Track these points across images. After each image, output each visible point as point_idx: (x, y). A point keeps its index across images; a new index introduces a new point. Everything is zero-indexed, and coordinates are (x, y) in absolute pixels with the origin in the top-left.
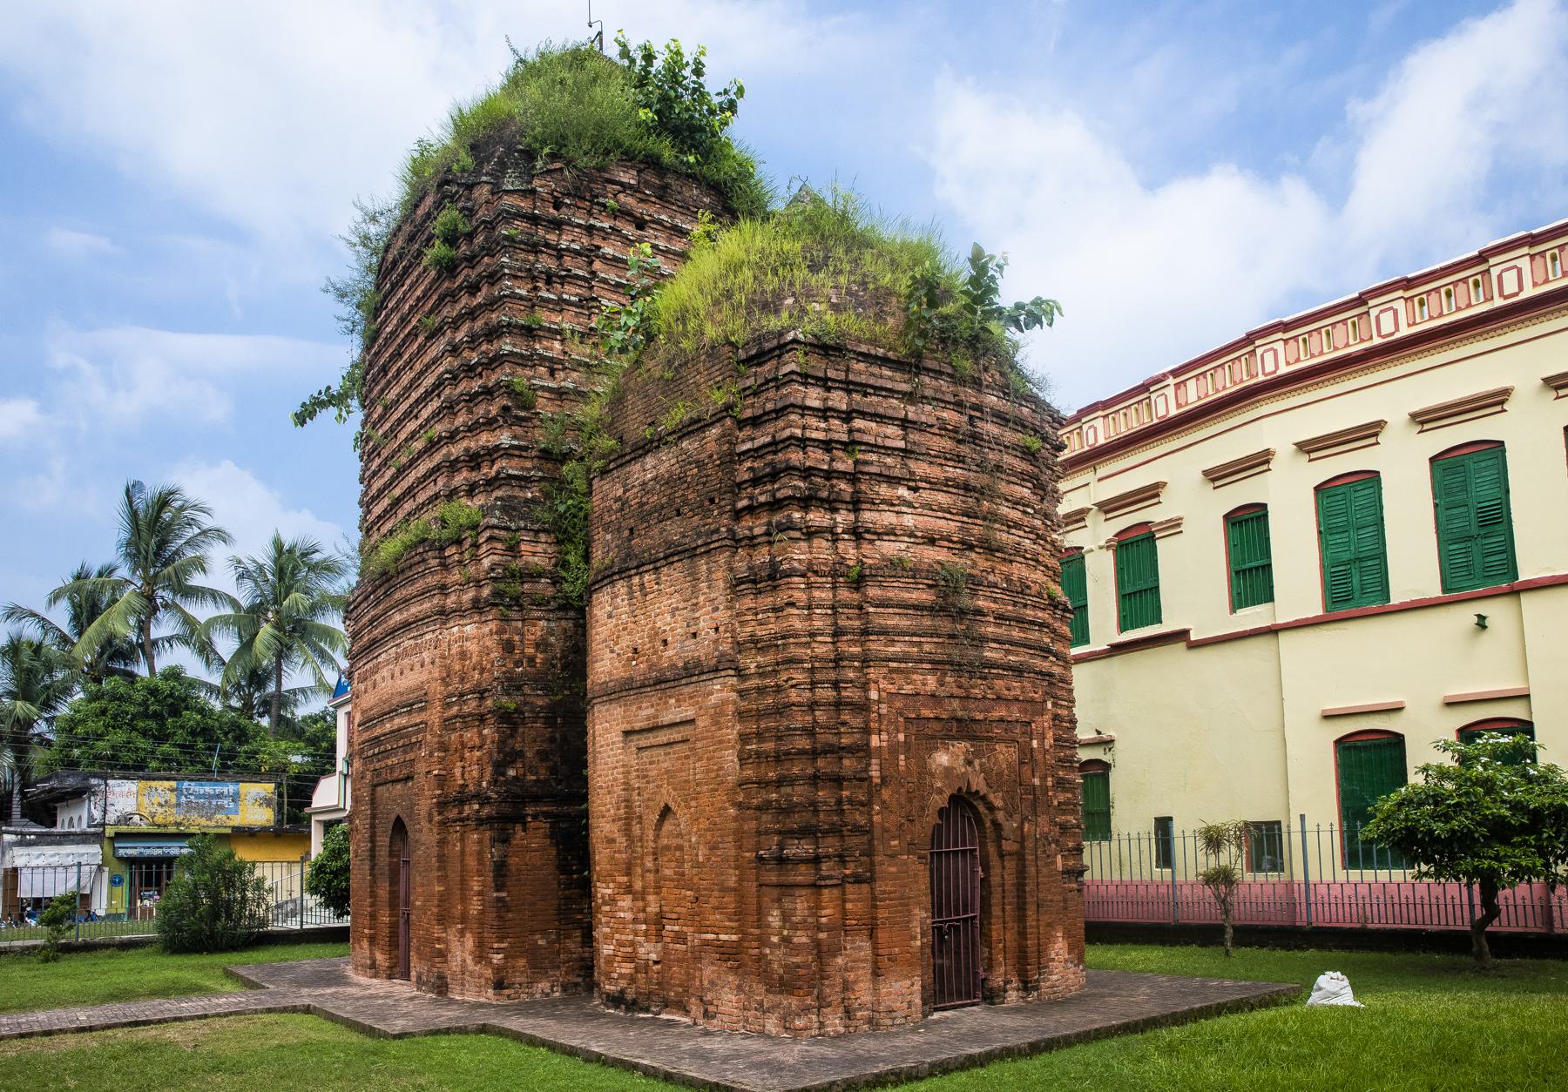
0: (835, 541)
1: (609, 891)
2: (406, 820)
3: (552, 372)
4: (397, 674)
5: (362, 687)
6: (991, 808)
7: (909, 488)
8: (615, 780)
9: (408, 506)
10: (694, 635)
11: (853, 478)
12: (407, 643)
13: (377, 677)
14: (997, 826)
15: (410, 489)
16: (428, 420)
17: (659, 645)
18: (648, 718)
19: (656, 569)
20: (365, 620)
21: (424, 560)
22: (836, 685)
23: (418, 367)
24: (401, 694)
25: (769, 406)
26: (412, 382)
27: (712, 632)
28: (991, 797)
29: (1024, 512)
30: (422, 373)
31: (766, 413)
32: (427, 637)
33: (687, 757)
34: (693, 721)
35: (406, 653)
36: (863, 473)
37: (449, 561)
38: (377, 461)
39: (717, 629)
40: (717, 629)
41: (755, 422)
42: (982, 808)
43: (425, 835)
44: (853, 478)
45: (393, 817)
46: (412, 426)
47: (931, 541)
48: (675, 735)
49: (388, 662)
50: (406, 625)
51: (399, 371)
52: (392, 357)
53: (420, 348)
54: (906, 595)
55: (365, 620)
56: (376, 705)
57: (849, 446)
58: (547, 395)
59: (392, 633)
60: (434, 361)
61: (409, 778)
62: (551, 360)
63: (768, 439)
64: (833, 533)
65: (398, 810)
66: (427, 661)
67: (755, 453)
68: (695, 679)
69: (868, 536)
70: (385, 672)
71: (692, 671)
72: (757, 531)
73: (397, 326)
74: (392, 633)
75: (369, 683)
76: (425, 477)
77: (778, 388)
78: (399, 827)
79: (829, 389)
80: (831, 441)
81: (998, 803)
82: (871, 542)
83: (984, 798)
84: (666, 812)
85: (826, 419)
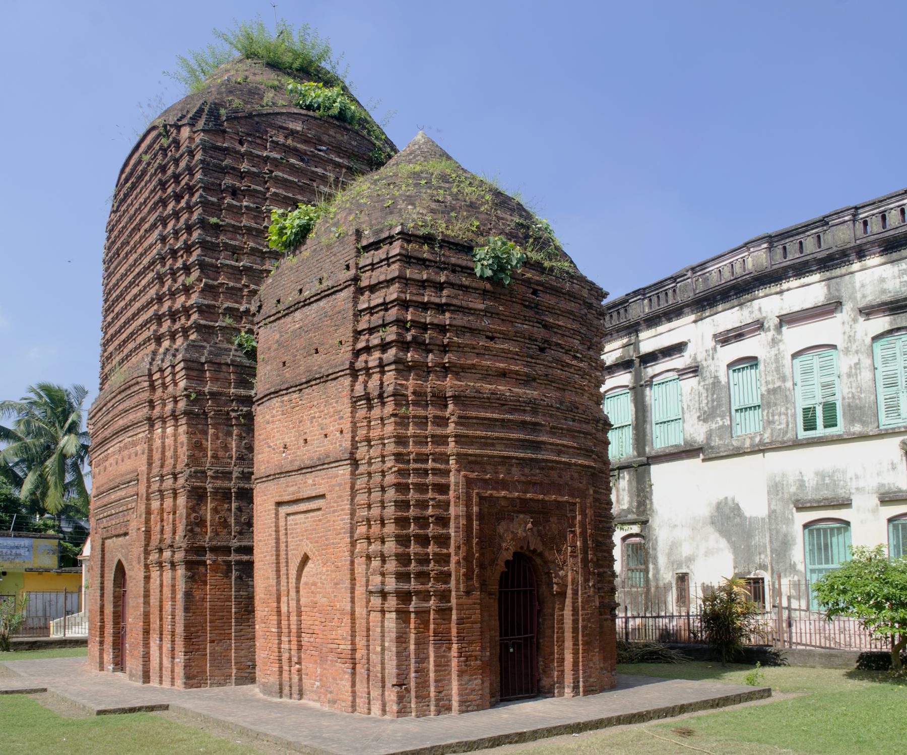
1: (265, 613)
2: (124, 563)
4: (120, 461)
5: (97, 470)
9: (131, 346)
10: (326, 436)
12: (127, 440)
13: (107, 463)
15: (132, 334)
16: (145, 287)
17: (302, 442)
18: (293, 494)
19: (300, 390)
20: (100, 424)
23: (140, 250)
24: (122, 475)
25: (382, 278)
26: (136, 261)
27: (338, 434)
30: (142, 255)
31: (380, 283)
32: (140, 436)
33: (320, 520)
35: (126, 447)
37: (156, 383)
38: (112, 315)
39: (341, 432)
40: (341, 432)
41: (373, 288)
43: (135, 574)
46: (135, 291)
49: (114, 453)
50: (125, 429)
51: (127, 254)
52: (123, 244)
53: (141, 238)
55: (100, 424)
56: (106, 483)
58: (230, 271)
59: (116, 433)
60: (150, 247)
61: (126, 534)
63: (381, 301)
65: (120, 556)
66: (139, 452)
67: (371, 310)
68: (326, 466)
70: (112, 460)
72: (371, 364)
73: (127, 223)
74: (116, 433)
75: (101, 467)
76: (142, 326)
77: (389, 265)
78: (120, 570)
84: (305, 559)
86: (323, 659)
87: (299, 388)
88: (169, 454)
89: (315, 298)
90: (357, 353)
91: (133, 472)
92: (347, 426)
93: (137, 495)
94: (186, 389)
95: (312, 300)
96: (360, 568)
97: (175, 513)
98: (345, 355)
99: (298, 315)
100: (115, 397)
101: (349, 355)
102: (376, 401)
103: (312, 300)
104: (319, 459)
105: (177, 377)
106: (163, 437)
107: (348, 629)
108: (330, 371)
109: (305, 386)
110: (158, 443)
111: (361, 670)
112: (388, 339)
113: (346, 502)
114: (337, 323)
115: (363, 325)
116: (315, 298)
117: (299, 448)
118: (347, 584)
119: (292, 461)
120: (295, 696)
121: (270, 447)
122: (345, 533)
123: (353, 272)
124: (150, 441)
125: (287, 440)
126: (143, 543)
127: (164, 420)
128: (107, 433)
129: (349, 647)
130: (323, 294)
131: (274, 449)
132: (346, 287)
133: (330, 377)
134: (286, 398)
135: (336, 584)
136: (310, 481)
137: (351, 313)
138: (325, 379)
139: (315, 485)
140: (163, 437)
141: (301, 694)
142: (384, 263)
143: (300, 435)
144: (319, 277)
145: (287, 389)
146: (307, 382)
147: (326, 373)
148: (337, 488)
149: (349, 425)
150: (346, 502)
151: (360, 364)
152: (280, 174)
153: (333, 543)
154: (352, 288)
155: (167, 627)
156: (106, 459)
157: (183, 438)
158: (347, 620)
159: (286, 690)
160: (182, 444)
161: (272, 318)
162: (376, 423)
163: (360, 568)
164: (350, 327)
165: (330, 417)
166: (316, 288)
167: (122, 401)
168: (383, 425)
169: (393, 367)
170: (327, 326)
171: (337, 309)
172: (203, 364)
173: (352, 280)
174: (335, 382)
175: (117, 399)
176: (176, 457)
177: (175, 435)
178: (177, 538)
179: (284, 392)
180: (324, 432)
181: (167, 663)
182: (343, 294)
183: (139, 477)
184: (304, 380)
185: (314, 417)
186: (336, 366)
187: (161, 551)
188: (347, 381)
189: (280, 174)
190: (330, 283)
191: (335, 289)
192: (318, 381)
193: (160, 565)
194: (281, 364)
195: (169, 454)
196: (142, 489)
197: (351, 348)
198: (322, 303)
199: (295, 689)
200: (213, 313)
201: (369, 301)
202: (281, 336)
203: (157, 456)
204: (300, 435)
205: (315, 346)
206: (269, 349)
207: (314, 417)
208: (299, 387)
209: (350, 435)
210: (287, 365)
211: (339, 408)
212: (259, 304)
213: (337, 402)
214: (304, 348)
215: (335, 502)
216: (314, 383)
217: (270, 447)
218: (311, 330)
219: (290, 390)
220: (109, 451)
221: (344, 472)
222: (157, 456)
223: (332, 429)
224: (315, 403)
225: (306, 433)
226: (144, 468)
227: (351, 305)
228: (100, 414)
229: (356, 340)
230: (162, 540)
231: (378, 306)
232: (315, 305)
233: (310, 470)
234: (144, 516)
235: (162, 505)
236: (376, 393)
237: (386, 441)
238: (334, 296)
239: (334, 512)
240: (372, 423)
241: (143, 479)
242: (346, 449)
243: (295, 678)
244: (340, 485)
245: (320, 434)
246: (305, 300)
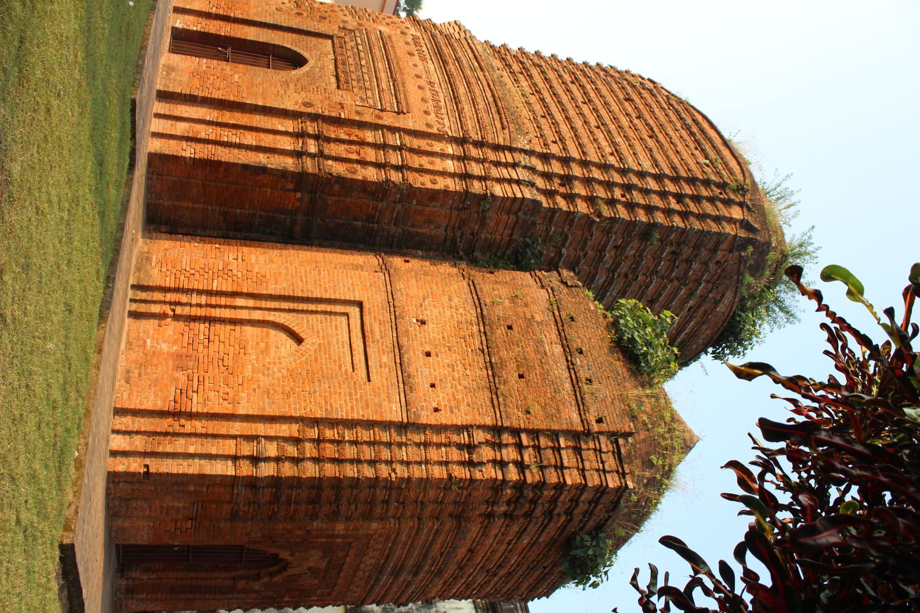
0: (487, 502)
3: (616, 247)
6: (271, 575)
7: (511, 540)
8: (326, 291)
9: (538, 108)
10: (433, 386)
11: (528, 515)
13: (417, 58)
14: (258, 577)
17: (427, 349)
19: (483, 351)
21: (503, 128)
22: (386, 502)
27: (435, 405)
28: (281, 576)
29: (474, 589)
31: (582, 461)
32: (446, 121)
34: (369, 380)
36: (530, 521)
39: (436, 410)
40: (436, 410)
42: (272, 569)
44: (528, 515)
45: (306, 55)
47: (471, 550)
48: (359, 357)
54: (440, 541)
57: (549, 514)
58: (603, 242)
62: (625, 248)
63: (566, 464)
64: (493, 503)
65: (311, 63)
68: (401, 385)
69: (486, 521)
71: (406, 382)
78: (297, 61)
79: (590, 503)
80: (556, 505)
81: (275, 579)
82: (482, 523)
83: (279, 572)
85: (571, 500)
86: (180, 361)
87: (486, 350)
88: (424, 161)
89: (574, 377)
90: (516, 432)
91: (408, 108)
92: (444, 418)
93: (382, 110)
94: (492, 195)
95: (572, 372)
96: (284, 430)
97: (358, 162)
98: (516, 419)
99: (558, 349)
100: (489, 86)
101: (515, 424)
102: (467, 456)
103: (572, 372)
104: (409, 376)
105: (506, 185)
106: (443, 156)
107: (217, 410)
108: (501, 399)
109: (488, 360)
110: (437, 147)
111: (164, 424)
112: (527, 473)
113: (361, 413)
114: (548, 407)
115: (544, 442)
116: (574, 377)
117: (422, 344)
118: (270, 411)
119: (407, 331)
120: (134, 307)
121: (424, 299)
122: (326, 410)
123: (595, 427)
124: (439, 137)
125: (431, 326)
126: (327, 113)
127: (463, 158)
128: (451, 67)
129: (194, 410)
130: (577, 389)
131: (421, 305)
132: (582, 421)
133: (494, 396)
134: (475, 328)
135: (268, 393)
136: (385, 359)
137: (555, 427)
138: (494, 391)
139: (381, 367)
140: (443, 156)
141: (135, 315)
142: (601, 465)
143: (436, 346)
144: (593, 379)
145: (485, 333)
146: (490, 362)
147: (499, 393)
148: (377, 401)
149: (444, 422)
150: (361, 413)
151: (507, 438)
152: (682, 293)
153: (315, 392)
154: (580, 428)
155: (227, 135)
156: (423, 59)
157: (442, 183)
158: (227, 408)
159: (143, 295)
160: (434, 182)
161: (556, 313)
162: (444, 454)
163: (284, 430)
164: (543, 426)
165: (453, 394)
166: (583, 374)
167: (485, 98)
168: (437, 464)
169: (500, 477)
170: (545, 393)
171: (561, 407)
172: (516, 214)
173: (589, 430)
174: (488, 403)
175: (487, 89)
176: (421, 171)
177: (444, 173)
178: (330, 162)
179: (482, 329)
180: (437, 383)
181: (181, 128)
182: (575, 417)
183: (402, 115)
184: (493, 360)
185: (453, 370)
186: (505, 405)
187: (317, 137)
188: (489, 421)
189: (682, 293)
190: (587, 397)
191: (581, 408)
192: (492, 380)
193: (300, 135)
194: (510, 323)
195: (424, 161)
196: (388, 119)
197: (522, 426)
198: (568, 385)
199: (143, 308)
200: (564, 223)
201: (567, 448)
202: (538, 323)
203: (423, 144)
204: (436, 346)
205: (526, 374)
206: (526, 305)
207: (453, 370)
208: (487, 350)
209: (434, 422)
210: (509, 331)
211: (462, 407)
212: (569, 284)
213: (468, 405)
214: (525, 359)
215: (361, 396)
216: (490, 373)
217: (424, 299)
218: (543, 369)
219: (484, 337)
220: (430, 62)
221: (394, 412)
222: (423, 144)
223: (440, 397)
224: (468, 372)
225: (437, 356)
226: (409, 123)
227: (565, 427)
228: (471, 55)
229: (529, 432)
230: (328, 140)
231: (561, 458)
232: (568, 374)
233: (398, 361)
234: (357, 118)
235: (369, 144)
236: (475, 457)
237: (423, 467)
238: (574, 402)
239: (350, 394)
240: (443, 449)
241: (401, 122)
242: (418, 416)
243: (156, 309)
244: (380, 406)
245: (435, 377)
246: (572, 364)
